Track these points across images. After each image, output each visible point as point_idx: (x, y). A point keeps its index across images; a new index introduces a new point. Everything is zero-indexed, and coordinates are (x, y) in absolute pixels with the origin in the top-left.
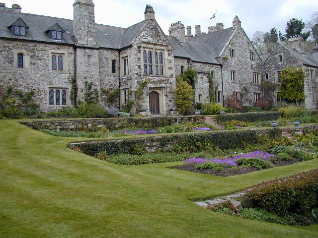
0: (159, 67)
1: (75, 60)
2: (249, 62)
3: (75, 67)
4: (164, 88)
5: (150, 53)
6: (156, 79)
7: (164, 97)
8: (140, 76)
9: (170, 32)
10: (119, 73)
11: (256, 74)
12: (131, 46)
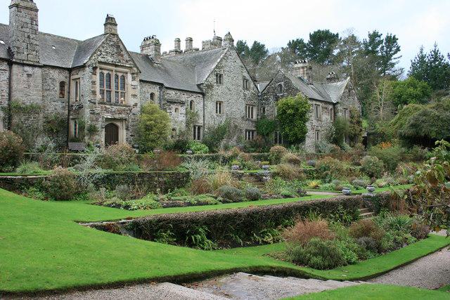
1: (10, 79)
3: (10, 88)
5: (109, 76)
6: (115, 108)
7: (125, 131)
9: (143, 47)
11: (249, 107)
12: (84, 66)
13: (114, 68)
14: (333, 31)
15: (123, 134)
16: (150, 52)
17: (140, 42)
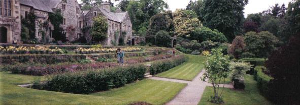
7: (11, 32)
11: (80, 23)
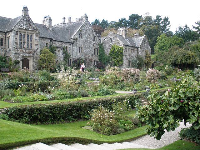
0: (29, 44)
2: (92, 42)
4: (32, 56)
5: (24, 35)
7: (32, 62)
8: (17, 49)
9: (43, 22)
10: (5, 46)
12: (11, 31)
13: (27, 31)
14: (139, 15)
15: (31, 64)
16: (47, 23)
17: (42, 19)
